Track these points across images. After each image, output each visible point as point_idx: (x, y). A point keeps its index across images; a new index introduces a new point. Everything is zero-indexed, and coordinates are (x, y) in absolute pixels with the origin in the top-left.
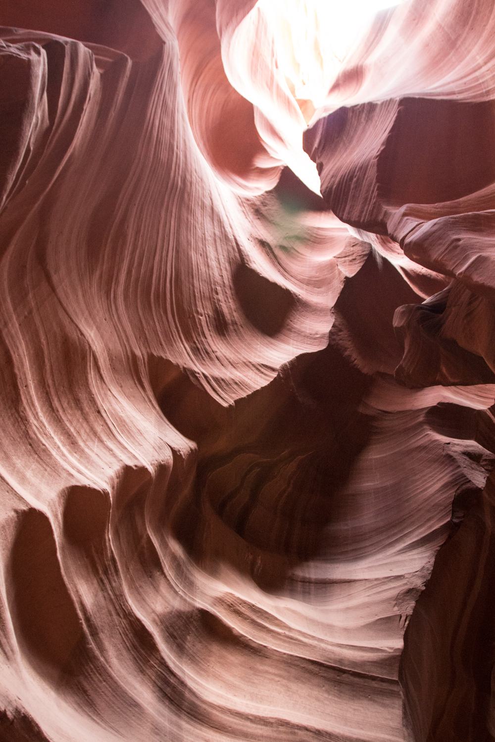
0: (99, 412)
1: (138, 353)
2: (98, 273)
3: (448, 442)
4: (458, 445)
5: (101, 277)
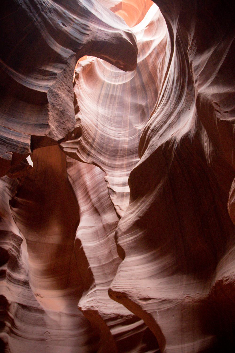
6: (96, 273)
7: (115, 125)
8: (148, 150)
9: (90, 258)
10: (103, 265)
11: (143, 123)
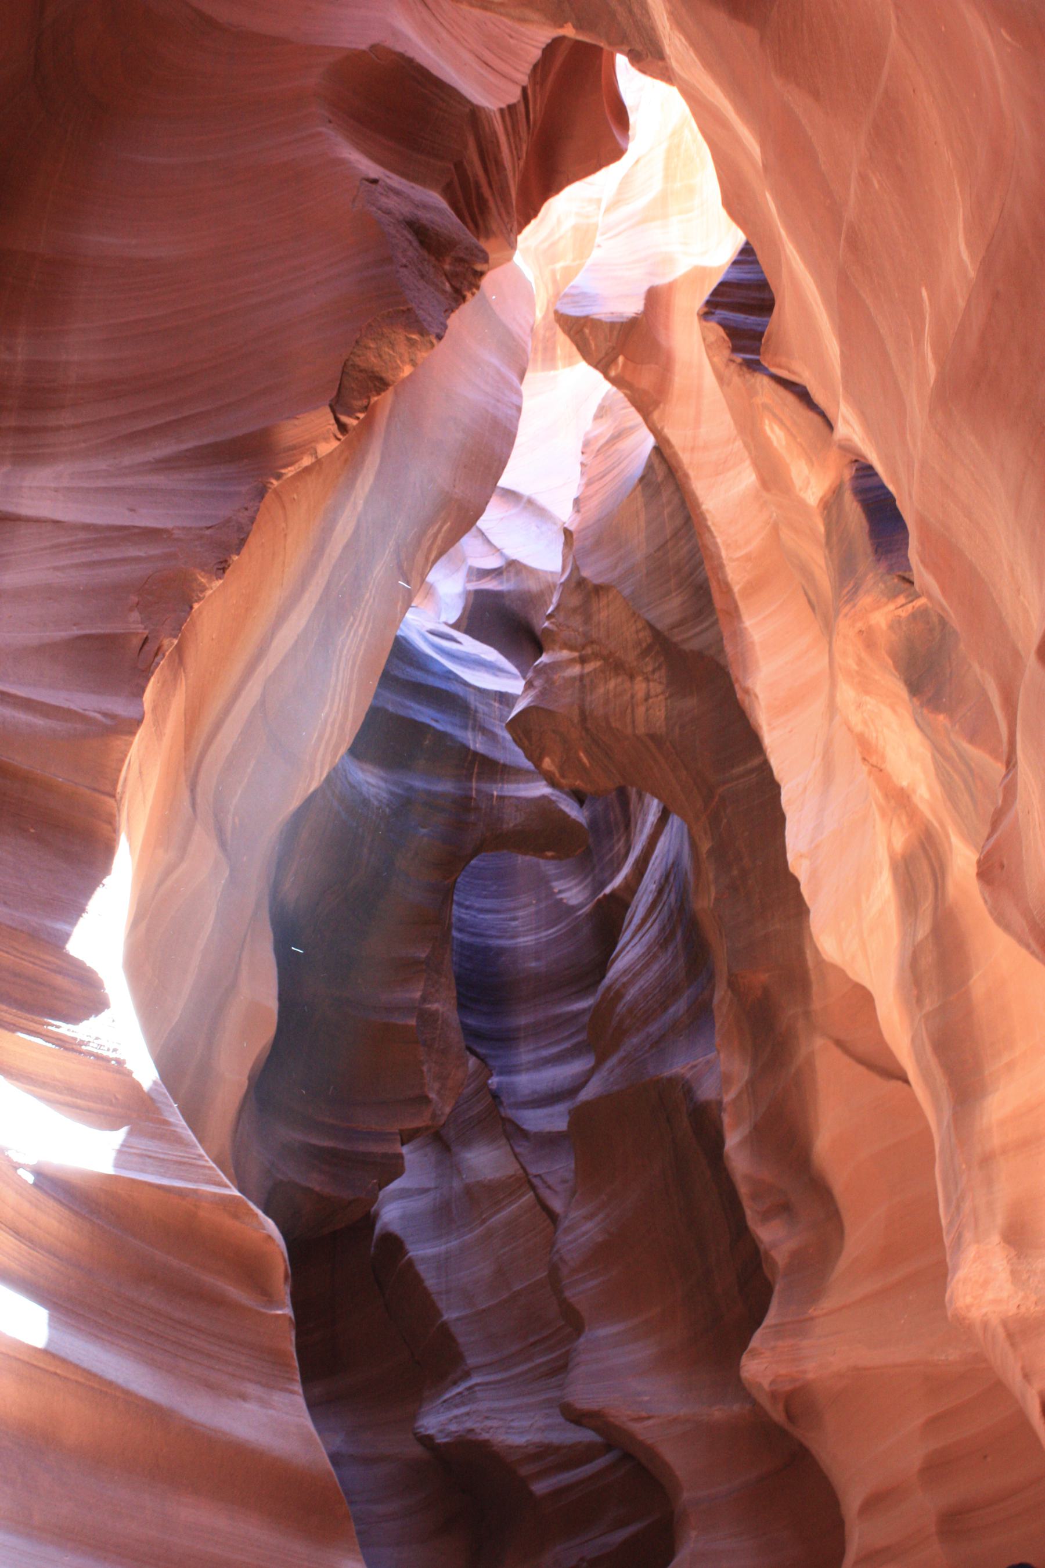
3: (373, 175)
4: (397, 193)
6: (464, 1338)
7: (495, 888)
8: (621, 1062)
9: (440, 1293)
10: (484, 1311)
11: (581, 882)
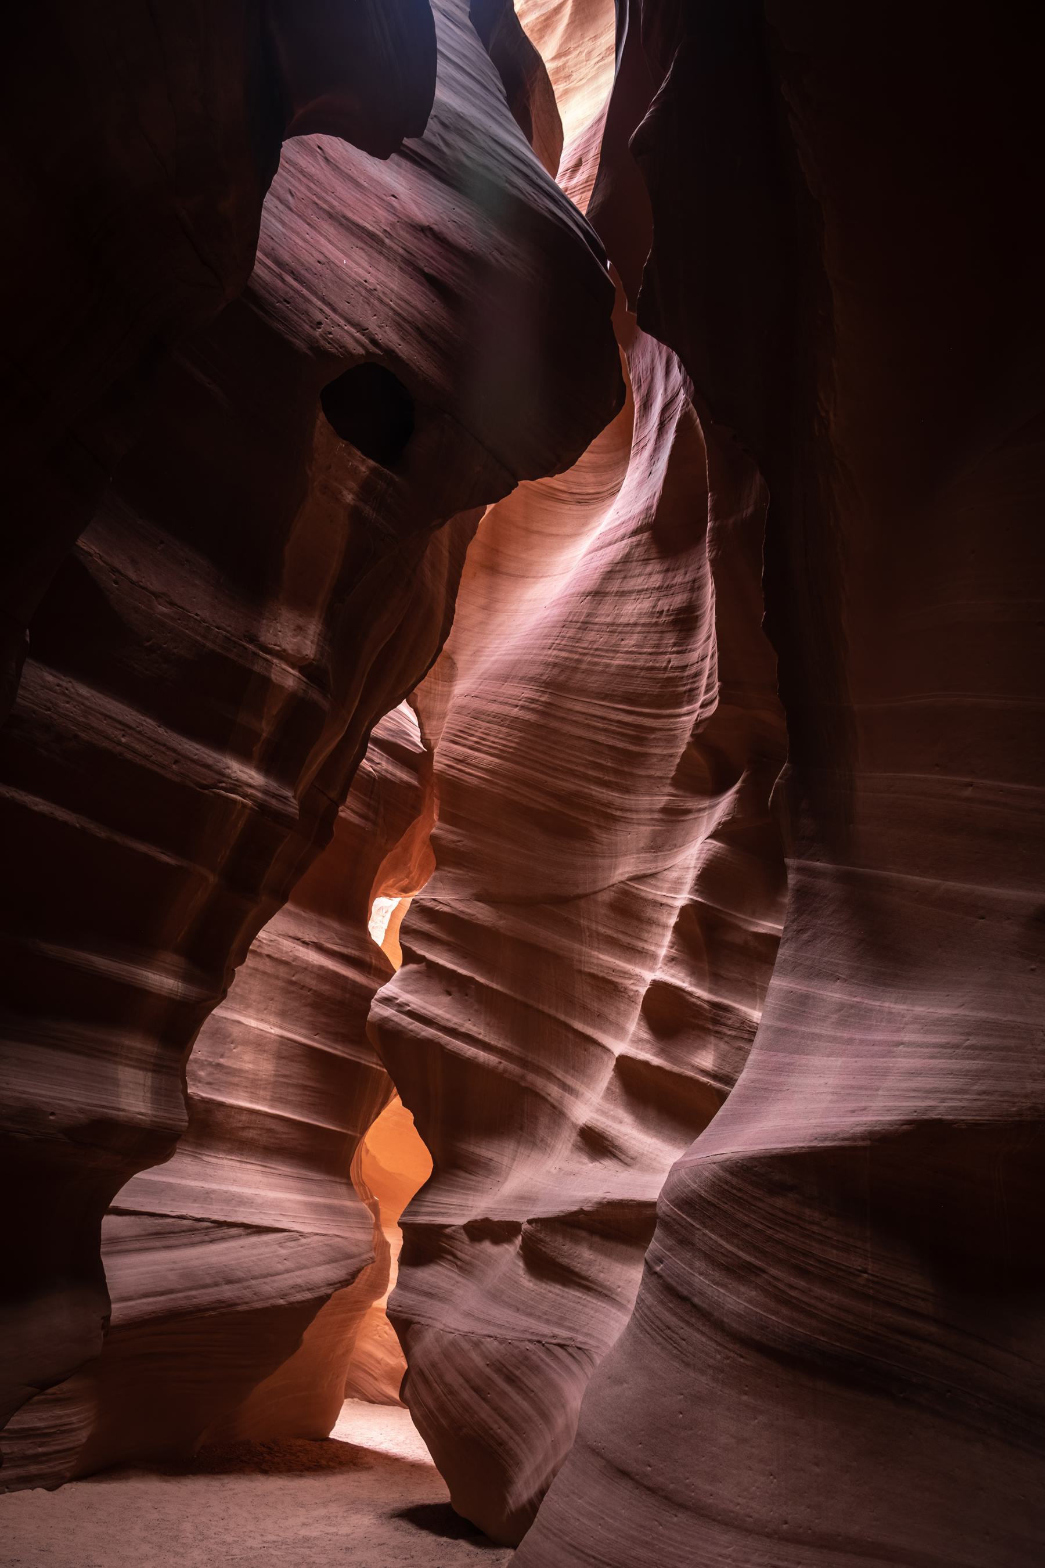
0: (662, 904)
1: (661, 801)
2: (596, 831)
5: (599, 827)
